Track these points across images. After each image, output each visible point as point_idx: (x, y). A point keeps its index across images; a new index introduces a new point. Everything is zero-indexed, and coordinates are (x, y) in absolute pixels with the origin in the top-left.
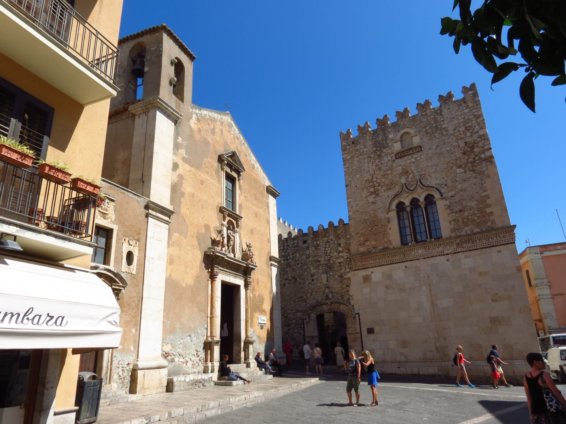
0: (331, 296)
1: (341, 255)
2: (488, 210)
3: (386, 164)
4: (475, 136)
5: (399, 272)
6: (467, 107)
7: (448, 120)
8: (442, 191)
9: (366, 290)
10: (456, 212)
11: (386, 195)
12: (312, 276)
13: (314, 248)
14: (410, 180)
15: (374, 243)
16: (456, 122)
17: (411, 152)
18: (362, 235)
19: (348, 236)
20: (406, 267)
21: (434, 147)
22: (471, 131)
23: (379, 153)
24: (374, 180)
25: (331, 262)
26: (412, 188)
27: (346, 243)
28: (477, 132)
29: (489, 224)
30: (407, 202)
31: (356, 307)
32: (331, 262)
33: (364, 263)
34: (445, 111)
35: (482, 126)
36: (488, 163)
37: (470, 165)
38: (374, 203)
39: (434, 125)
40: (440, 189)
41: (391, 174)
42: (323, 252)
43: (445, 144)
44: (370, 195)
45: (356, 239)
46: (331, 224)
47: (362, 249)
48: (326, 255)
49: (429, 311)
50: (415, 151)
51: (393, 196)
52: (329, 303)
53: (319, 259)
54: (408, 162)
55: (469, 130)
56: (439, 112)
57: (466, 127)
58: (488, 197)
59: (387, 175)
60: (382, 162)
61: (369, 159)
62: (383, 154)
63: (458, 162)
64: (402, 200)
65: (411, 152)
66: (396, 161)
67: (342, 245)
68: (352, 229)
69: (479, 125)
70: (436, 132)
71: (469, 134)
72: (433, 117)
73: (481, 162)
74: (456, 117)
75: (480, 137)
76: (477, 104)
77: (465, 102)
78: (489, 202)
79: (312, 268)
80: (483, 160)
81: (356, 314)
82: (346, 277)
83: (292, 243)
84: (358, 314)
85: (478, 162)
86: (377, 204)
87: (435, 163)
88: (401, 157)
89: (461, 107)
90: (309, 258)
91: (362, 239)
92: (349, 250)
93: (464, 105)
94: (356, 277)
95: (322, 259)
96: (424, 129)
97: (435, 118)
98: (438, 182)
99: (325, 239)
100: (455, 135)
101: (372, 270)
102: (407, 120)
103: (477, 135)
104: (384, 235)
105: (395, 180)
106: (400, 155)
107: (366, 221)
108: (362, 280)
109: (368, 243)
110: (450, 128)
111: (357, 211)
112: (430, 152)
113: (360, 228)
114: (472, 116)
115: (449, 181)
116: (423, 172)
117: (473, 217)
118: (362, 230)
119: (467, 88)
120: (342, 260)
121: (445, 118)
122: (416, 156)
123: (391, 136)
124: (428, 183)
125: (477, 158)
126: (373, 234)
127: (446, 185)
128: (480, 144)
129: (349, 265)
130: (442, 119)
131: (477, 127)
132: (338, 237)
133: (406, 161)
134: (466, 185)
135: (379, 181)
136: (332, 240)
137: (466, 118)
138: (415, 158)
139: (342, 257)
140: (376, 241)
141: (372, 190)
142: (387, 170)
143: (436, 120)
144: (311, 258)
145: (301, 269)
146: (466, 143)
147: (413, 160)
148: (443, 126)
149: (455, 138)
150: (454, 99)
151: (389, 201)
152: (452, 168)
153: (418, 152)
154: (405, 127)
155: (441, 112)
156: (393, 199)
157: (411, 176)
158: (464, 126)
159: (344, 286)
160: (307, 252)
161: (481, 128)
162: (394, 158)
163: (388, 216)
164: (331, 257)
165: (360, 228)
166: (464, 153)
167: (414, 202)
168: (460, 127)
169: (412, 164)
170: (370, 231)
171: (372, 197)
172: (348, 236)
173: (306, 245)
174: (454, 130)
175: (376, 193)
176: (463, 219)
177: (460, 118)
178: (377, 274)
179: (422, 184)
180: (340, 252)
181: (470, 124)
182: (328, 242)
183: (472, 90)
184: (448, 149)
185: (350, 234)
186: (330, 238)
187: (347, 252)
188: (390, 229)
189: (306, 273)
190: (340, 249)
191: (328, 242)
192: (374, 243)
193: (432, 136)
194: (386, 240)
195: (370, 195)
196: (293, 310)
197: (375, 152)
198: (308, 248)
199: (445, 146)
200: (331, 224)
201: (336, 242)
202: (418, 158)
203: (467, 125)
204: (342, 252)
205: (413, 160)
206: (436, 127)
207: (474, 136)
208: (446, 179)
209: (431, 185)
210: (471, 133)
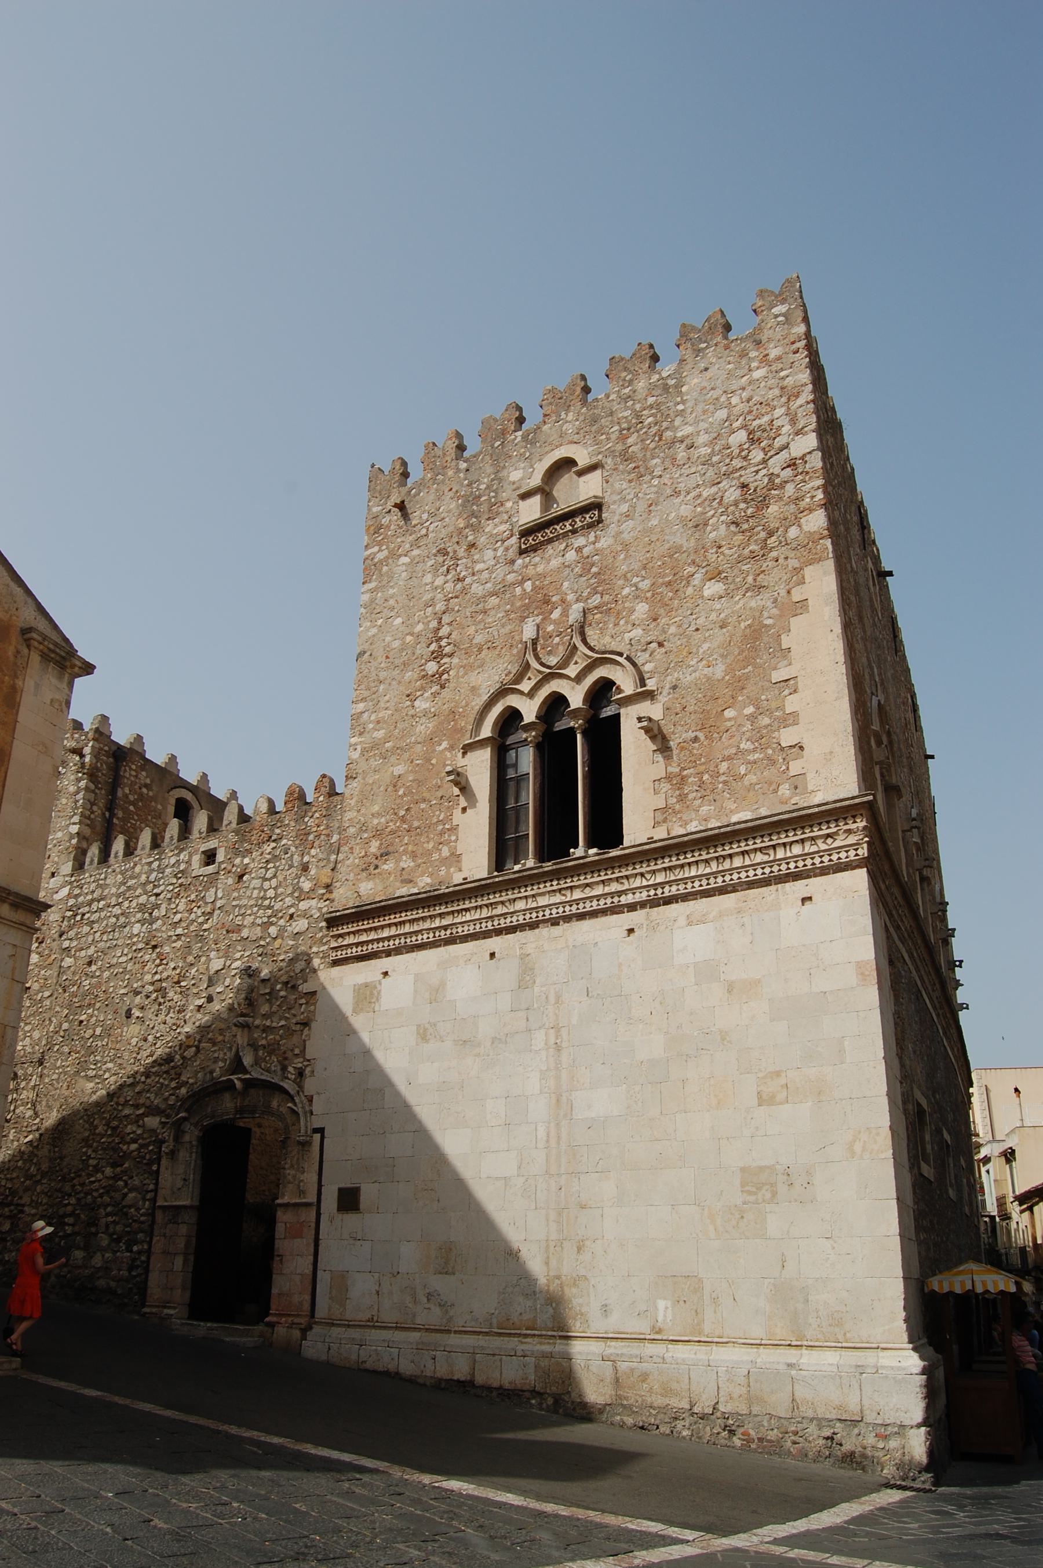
1: (303, 905)
2: (787, 737)
3: (485, 575)
4: (776, 463)
6: (765, 359)
15: (407, 863)
18: (378, 833)
21: (641, 507)
23: (470, 538)
24: (444, 631)
29: (785, 790)
31: (317, 1107)
39: (654, 430)
42: (256, 893)
43: (677, 493)
49: (541, 1133)
53: (238, 921)
54: (555, 563)
55: (759, 440)
60: (479, 567)
61: (440, 559)
62: (482, 540)
63: (712, 556)
66: (520, 561)
67: (313, 872)
78: (792, 704)
79: (213, 954)
81: (316, 1131)
83: (173, 860)
84: (321, 1131)
90: (211, 914)
91: (374, 847)
93: (753, 354)
99: (268, 848)
101: (384, 963)
104: (442, 833)
109: (388, 866)
114: (777, 392)
120: (301, 925)
122: (579, 541)
123: (515, 475)
127: (660, 645)
128: (790, 489)
137: (756, 398)
138: (579, 550)
139: (305, 915)
140: (414, 856)
141: (432, 667)
149: (711, 473)
153: (591, 526)
157: (556, 615)
158: (744, 427)
162: (512, 553)
163: (460, 762)
170: (403, 819)
173: (211, 869)
174: (712, 443)
177: (735, 400)
185: (341, 830)
186: (284, 842)
192: (407, 863)
196: (137, 1106)
197: (460, 531)
199: (677, 501)
202: (586, 551)
205: (571, 555)
207: (771, 462)
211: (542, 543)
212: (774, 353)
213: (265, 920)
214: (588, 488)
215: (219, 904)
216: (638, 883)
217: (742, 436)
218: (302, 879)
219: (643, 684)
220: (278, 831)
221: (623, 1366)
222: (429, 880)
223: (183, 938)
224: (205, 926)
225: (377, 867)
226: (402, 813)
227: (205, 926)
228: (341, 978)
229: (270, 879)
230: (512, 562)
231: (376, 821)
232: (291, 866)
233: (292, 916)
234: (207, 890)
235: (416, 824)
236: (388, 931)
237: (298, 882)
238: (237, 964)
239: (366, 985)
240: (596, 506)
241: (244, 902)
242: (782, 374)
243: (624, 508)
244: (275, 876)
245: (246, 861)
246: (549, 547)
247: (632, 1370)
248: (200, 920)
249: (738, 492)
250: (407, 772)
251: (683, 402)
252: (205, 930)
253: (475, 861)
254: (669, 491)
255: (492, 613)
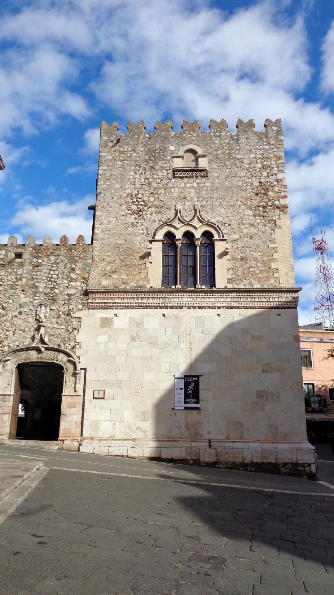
0: (46, 340)
1: (73, 284)
2: (274, 265)
5: (152, 319)
6: (269, 143)
7: (245, 151)
8: (224, 231)
9: (103, 338)
10: (236, 260)
11: (152, 220)
12: (21, 306)
13: (31, 267)
14: (186, 208)
15: (124, 277)
16: (253, 156)
17: (194, 175)
18: (109, 263)
19: (89, 261)
20: (164, 315)
21: (223, 177)
22: (268, 171)
25: (56, 291)
26: (187, 219)
27: (84, 270)
28: (275, 174)
29: (272, 281)
30: (179, 235)
32: (56, 291)
33: (106, 301)
34: (243, 140)
35: (282, 169)
36: (281, 212)
37: (261, 209)
38: (133, 225)
39: (227, 152)
40: (222, 228)
41: (164, 194)
42: (46, 275)
43: (236, 176)
44: (130, 214)
45: (100, 267)
46: (64, 239)
47: (106, 283)
48: (49, 281)
50: (198, 175)
51: (162, 223)
52: (43, 349)
53: (37, 284)
55: (266, 169)
56: (235, 138)
57: (263, 166)
58: (275, 250)
59: (158, 194)
64: (173, 230)
65: (194, 175)
66: (173, 180)
67: (77, 272)
68: (96, 253)
69: (278, 167)
70: (228, 161)
71: (265, 174)
72: (228, 141)
73: (274, 209)
74: (254, 151)
75: (277, 180)
76: (280, 143)
77: (266, 137)
78: (275, 256)
80: (277, 208)
82: (76, 315)
85: (269, 207)
86: (138, 228)
87: (221, 196)
88: (180, 177)
89: (261, 141)
90: (20, 279)
91: (109, 268)
92: (87, 280)
93: (265, 140)
94: (90, 318)
95: (43, 285)
96: (215, 153)
97: (229, 143)
98: (221, 219)
100: (251, 170)
102: (195, 135)
103: (274, 177)
104: (141, 269)
105: (169, 203)
106: (178, 173)
107: (118, 246)
108: (99, 322)
109: (115, 276)
110: (246, 161)
111: (107, 230)
112: (216, 181)
113: (109, 254)
114: (272, 155)
115: (233, 221)
116: (204, 203)
117: (255, 269)
118: (109, 256)
119: (272, 122)
120: (72, 291)
121: (242, 147)
122: (199, 181)
124: (209, 218)
125: (270, 203)
126: (126, 265)
129: (82, 300)
130: (238, 148)
131: (276, 169)
132: (72, 259)
133: (185, 184)
134: (253, 230)
135: (145, 199)
136: (62, 261)
137: (265, 155)
138: (198, 184)
139: (73, 287)
140: (128, 275)
142: (159, 188)
143: (230, 147)
144: (24, 280)
145: (4, 295)
146: (261, 183)
147: (195, 185)
148: (239, 156)
149: (248, 174)
150: (256, 129)
151: (155, 228)
152: (240, 206)
153: (203, 177)
154: (192, 142)
155: (238, 140)
156: (161, 226)
159: (70, 329)
160: (20, 271)
161: (279, 171)
162: (170, 176)
164: (57, 284)
165: (109, 254)
166: (257, 194)
167: (188, 235)
168: (257, 163)
169: (192, 190)
171: (133, 217)
172: (89, 261)
175: (139, 213)
176: (243, 270)
177: (258, 153)
178: (123, 318)
179: (200, 216)
180: (72, 280)
181: (269, 163)
182: (56, 263)
183: (276, 126)
184: (240, 184)
187: (82, 282)
188: (151, 263)
189: (11, 301)
190: (73, 276)
191: (56, 263)
192: (124, 277)
193: (223, 164)
194: (142, 276)
195: (130, 214)
198: (21, 265)
199: (237, 179)
200: (64, 239)
201: (68, 266)
203: (265, 163)
204: (75, 280)
205: (195, 185)
206: (230, 154)
208: (231, 218)
209: (212, 221)
210: (268, 174)
211: (183, 177)
212: (272, 142)
213: (52, 286)
214: (203, 163)
215: (24, 275)
216: (221, 300)
217: (260, 166)
218: (72, 273)
219: (223, 237)
220: (58, 253)
221: (219, 450)
222: (135, 285)
223: (3, 286)
224: (17, 283)
225: (110, 276)
226: (122, 258)
227: (17, 283)
228: (94, 314)
229: (54, 271)
230: (171, 180)
231: (109, 259)
232: (65, 268)
233: (67, 287)
234: (17, 269)
235: (129, 263)
236: (117, 300)
237: (69, 275)
238: (37, 301)
239: (106, 318)
240: (204, 170)
241: (38, 277)
242: (275, 150)
243: (216, 175)
244: (56, 270)
245: (40, 261)
246: (186, 179)
247: (222, 451)
248: (15, 280)
249: (258, 184)
250: (124, 243)
251: (239, 146)
252: (17, 285)
253: (156, 282)
254: (234, 175)
255: (162, 195)
